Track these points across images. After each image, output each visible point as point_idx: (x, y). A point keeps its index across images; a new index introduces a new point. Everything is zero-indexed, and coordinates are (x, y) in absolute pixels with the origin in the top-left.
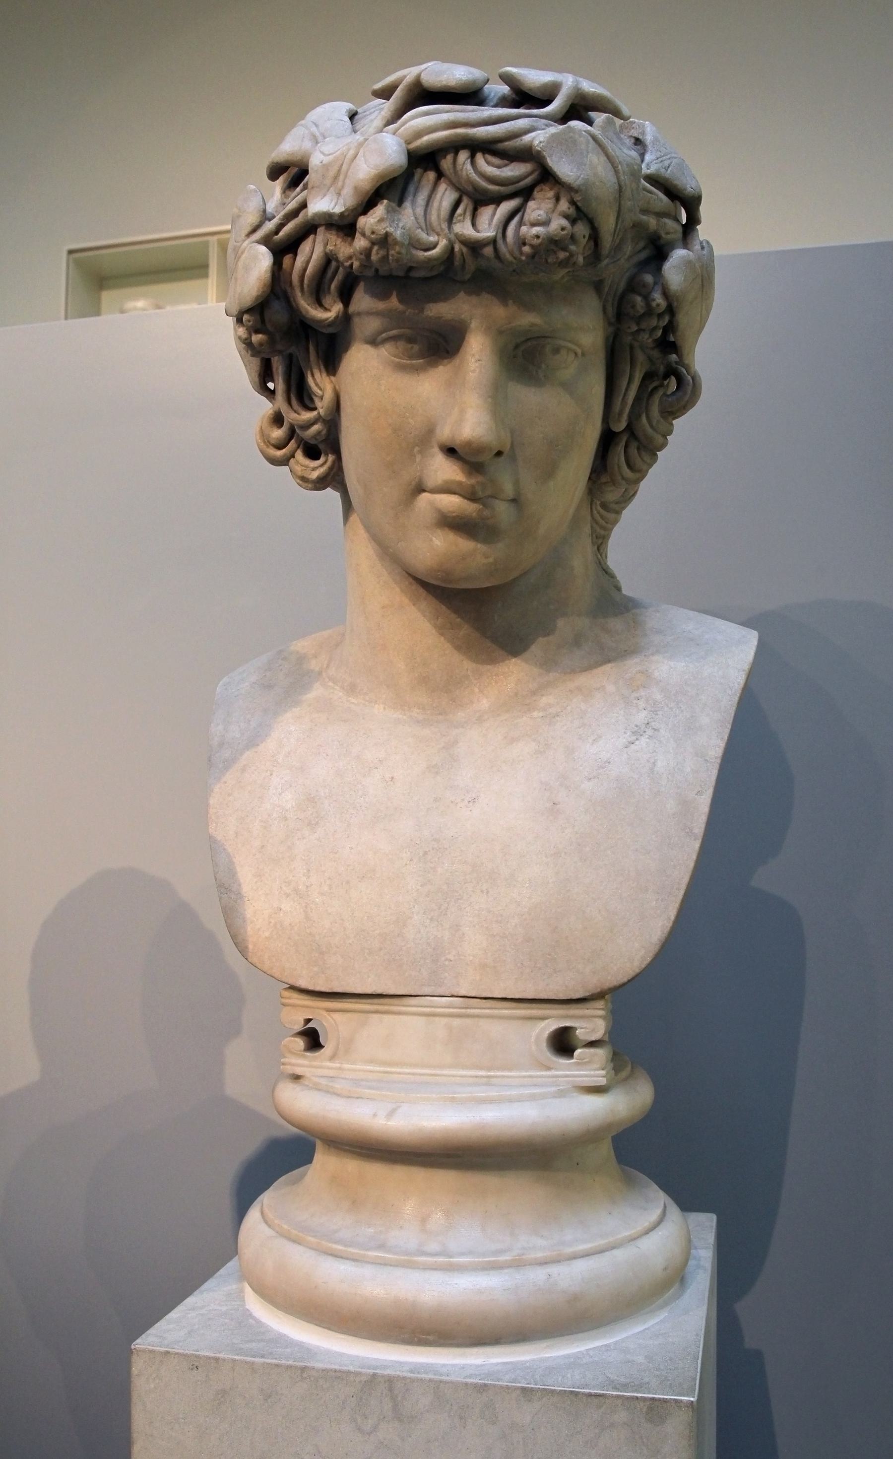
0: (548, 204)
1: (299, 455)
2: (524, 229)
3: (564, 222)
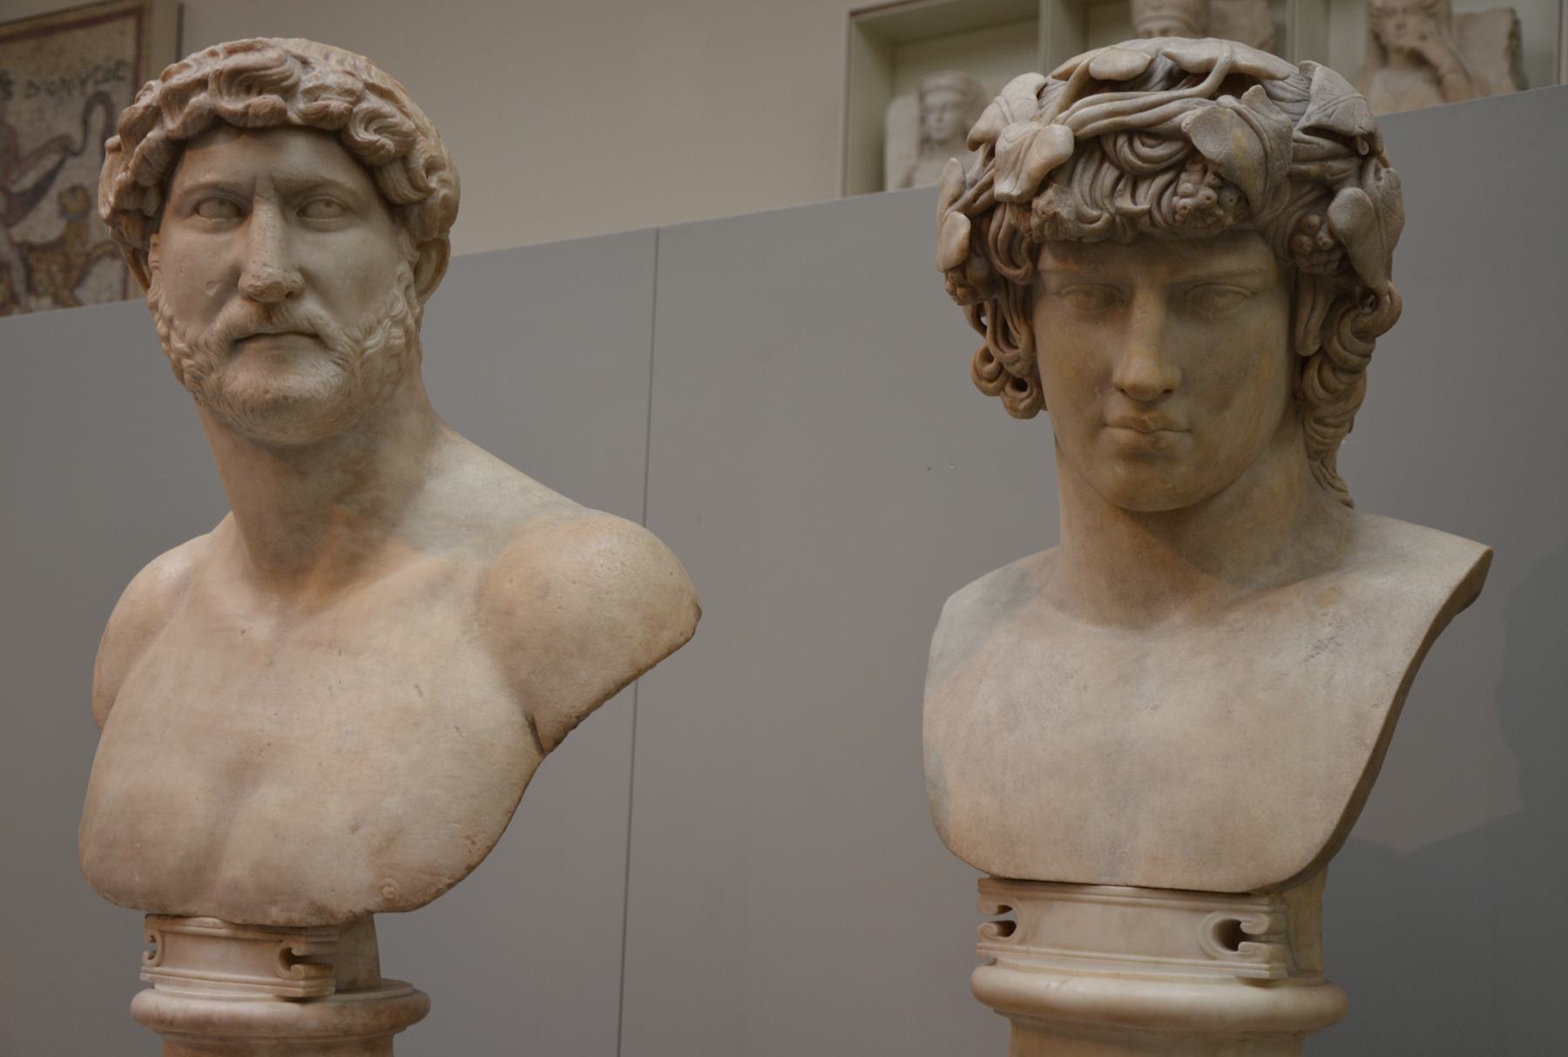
0: (1196, 177)
1: (1008, 389)
2: (1175, 199)
3: (1210, 192)
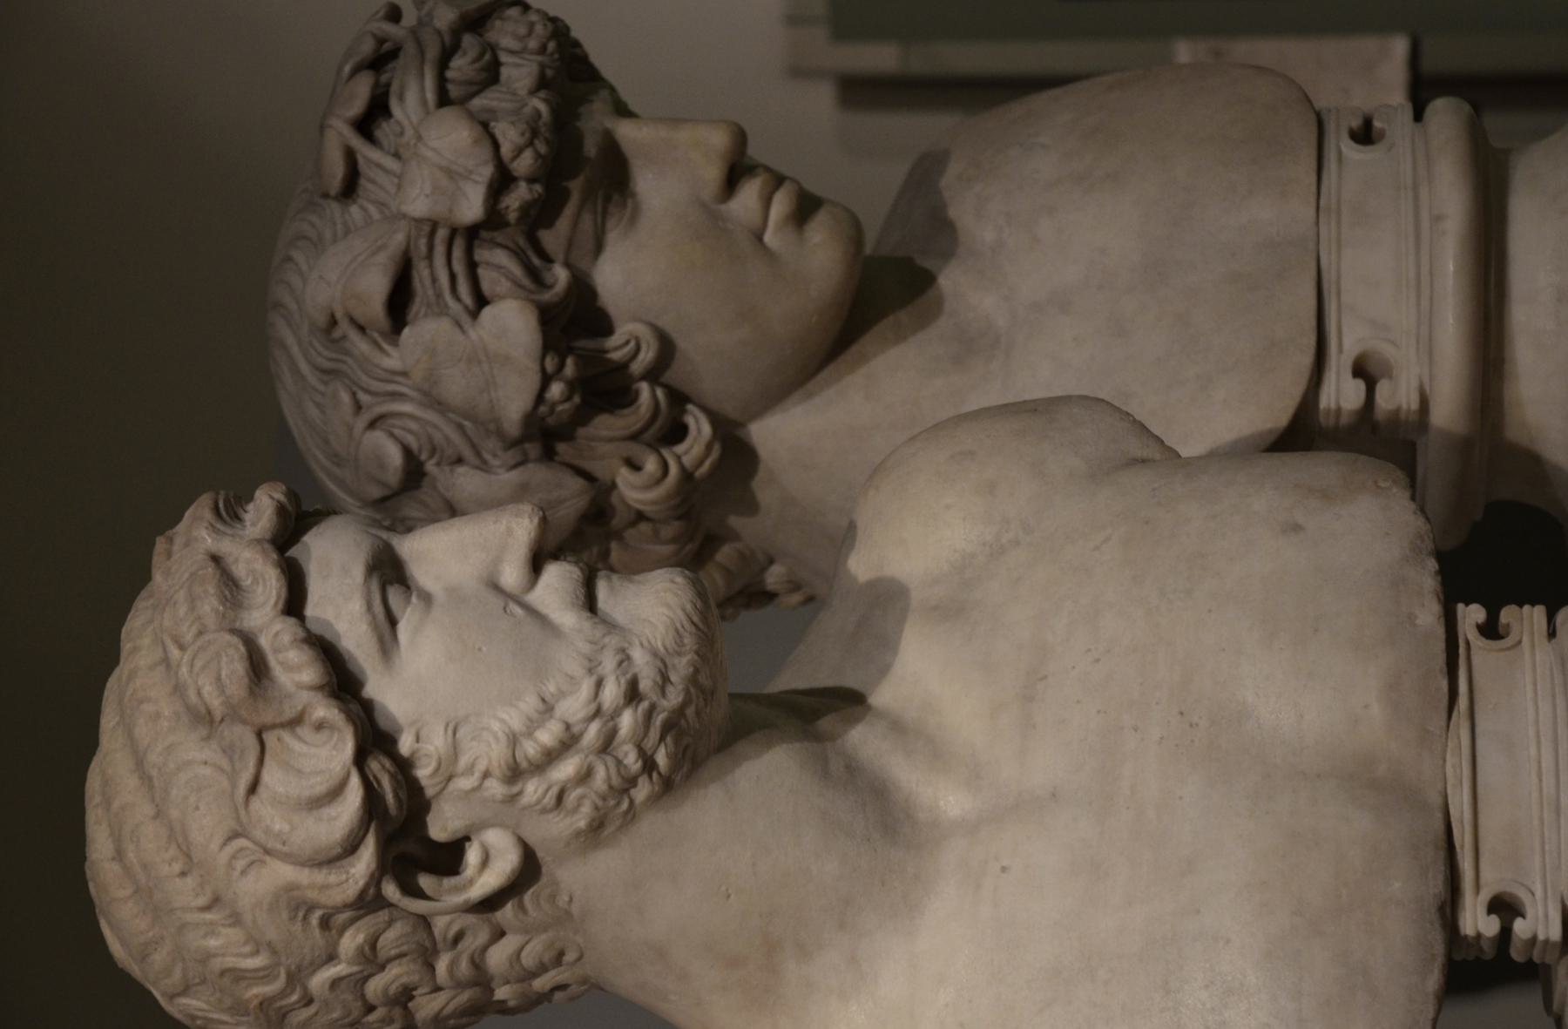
1: (680, 449)
